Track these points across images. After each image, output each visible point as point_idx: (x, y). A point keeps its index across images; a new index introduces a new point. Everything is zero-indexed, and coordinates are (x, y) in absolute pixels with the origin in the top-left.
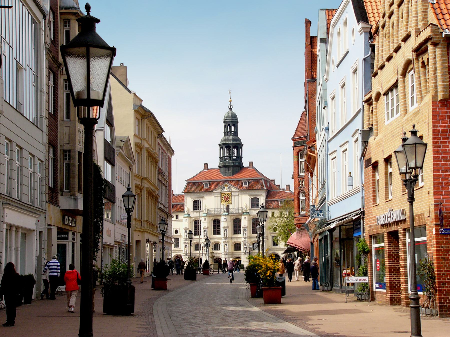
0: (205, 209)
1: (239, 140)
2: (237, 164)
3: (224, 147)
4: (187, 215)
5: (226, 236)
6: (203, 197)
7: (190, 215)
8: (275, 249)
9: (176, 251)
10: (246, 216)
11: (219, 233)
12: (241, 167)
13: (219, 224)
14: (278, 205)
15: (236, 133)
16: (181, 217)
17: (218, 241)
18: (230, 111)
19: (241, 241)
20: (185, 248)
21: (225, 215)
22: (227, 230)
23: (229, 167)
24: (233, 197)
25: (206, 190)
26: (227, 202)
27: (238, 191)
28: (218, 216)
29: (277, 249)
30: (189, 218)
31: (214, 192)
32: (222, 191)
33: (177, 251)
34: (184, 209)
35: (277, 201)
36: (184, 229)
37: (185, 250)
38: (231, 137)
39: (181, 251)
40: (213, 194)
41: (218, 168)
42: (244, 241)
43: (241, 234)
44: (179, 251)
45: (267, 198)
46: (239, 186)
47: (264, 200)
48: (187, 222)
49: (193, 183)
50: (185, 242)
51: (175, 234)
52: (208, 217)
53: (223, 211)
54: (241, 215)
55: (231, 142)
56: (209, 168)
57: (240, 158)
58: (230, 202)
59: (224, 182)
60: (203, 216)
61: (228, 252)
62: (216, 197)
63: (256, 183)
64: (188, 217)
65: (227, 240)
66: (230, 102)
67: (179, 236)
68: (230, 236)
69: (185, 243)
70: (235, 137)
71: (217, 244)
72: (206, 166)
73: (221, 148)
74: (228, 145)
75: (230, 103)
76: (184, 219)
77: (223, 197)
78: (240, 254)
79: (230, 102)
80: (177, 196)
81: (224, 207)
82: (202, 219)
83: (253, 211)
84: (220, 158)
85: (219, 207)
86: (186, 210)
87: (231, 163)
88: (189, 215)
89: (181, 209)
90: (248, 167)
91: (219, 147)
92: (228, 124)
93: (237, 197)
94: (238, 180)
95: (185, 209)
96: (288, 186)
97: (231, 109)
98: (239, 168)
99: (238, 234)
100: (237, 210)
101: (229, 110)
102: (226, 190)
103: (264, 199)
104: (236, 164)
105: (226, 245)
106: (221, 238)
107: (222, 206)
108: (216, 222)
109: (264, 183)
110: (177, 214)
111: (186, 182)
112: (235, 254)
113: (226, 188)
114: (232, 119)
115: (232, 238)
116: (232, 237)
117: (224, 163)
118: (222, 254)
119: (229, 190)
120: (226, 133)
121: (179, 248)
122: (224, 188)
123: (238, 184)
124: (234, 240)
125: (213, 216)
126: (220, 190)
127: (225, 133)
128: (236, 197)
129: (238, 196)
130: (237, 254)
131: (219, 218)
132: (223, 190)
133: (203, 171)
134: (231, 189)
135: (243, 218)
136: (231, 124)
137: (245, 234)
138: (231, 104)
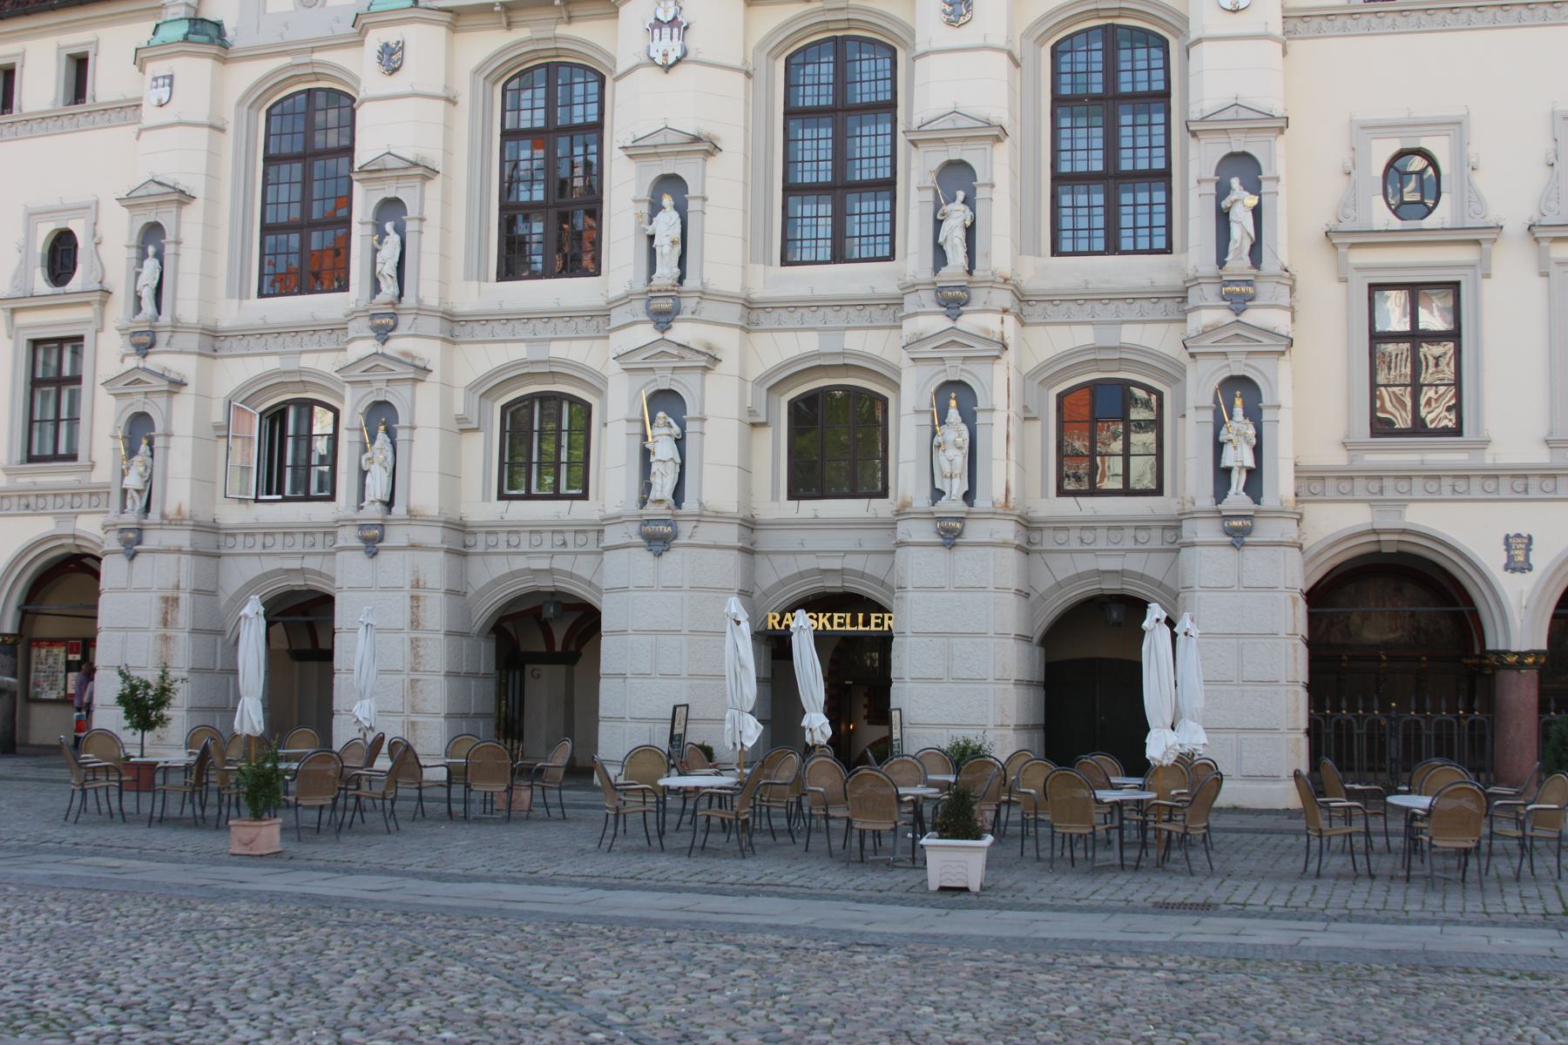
5: (667, 269)
7: (218, 26)
8: (1405, 476)
17: (558, 350)
20: (132, 452)
29: (1434, 476)
36: (130, 201)
37: (133, 481)
50: (132, 380)
52: (439, 32)
105: (666, 401)
110: (76, 40)
112: (790, 540)
116: (759, 292)
118: (613, 536)
130: (814, 541)
137: (953, 235)
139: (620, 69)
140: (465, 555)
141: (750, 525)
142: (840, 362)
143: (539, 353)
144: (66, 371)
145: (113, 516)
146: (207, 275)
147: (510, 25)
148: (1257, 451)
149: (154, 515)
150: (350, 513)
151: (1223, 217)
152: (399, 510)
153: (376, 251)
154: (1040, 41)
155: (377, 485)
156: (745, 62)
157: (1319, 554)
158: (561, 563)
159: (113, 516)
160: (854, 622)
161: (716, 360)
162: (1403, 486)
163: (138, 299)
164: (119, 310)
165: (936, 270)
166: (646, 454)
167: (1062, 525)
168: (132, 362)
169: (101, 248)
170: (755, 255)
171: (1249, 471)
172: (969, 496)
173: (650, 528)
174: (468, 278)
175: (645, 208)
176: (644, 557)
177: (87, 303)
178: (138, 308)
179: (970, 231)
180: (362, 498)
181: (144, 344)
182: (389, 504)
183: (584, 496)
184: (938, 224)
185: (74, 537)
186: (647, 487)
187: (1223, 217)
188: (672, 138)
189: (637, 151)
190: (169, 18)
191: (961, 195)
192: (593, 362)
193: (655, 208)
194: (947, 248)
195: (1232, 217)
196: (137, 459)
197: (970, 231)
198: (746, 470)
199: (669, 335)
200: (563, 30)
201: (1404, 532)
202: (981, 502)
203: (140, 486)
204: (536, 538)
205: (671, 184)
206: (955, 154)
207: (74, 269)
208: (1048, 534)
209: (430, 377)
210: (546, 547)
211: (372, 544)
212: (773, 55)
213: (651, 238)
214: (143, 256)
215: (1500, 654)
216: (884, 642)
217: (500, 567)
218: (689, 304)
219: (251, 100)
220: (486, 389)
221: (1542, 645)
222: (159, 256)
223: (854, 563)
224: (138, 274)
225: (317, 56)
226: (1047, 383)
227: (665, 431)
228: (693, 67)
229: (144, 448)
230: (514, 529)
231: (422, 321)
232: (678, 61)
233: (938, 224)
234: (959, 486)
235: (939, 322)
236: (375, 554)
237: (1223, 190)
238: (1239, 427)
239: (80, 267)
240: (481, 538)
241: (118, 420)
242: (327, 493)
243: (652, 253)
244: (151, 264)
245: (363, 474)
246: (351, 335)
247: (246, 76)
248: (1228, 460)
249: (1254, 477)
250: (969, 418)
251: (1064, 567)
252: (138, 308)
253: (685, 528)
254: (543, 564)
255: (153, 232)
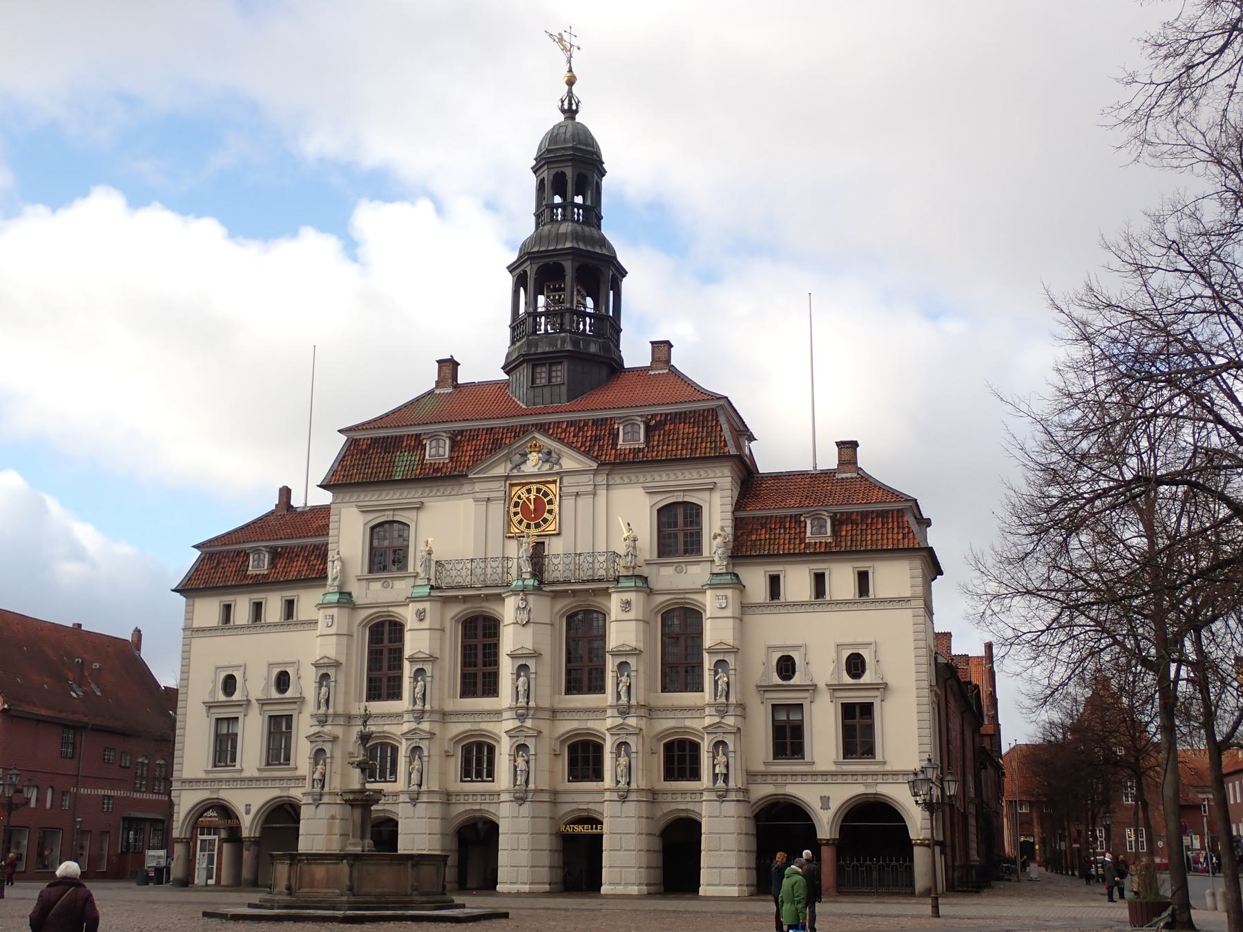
0: (427, 564)
1: (603, 242)
2: (593, 348)
3: (530, 269)
4: (335, 598)
6: (420, 507)
7: (350, 594)
8: (784, 774)
9: (274, 779)
10: (631, 596)
11: (491, 689)
12: (613, 366)
13: (491, 641)
14: (802, 540)
15: (593, 215)
16: (308, 602)
18: (570, 122)
19: (604, 726)
20: (316, 763)
21: (524, 590)
22: (532, 670)
23: (550, 360)
24: (568, 503)
25: (436, 470)
26: (537, 526)
27: (596, 472)
28: (488, 597)
29: (794, 775)
30: (346, 612)
31: (472, 481)
32: (515, 472)
33: (281, 779)
34: (325, 570)
35: (796, 519)
37: (317, 776)
38: (565, 228)
39: (297, 779)
40: (466, 488)
41: (507, 377)
42: (620, 727)
43: (601, 689)
44: (289, 779)
45: (739, 506)
46: (601, 448)
47: (729, 515)
48: (333, 630)
49: (375, 440)
50: (318, 735)
51: (275, 694)
52: (438, 605)
53: (514, 571)
54: (606, 593)
55: (568, 245)
56: (460, 381)
57: (609, 327)
58: (552, 528)
59: (525, 430)
60: (413, 599)
61: (531, 786)
62: (483, 505)
63: (684, 429)
64: (339, 604)
65: (529, 723)
66: (571, 82)
67: (293, 701)
68: (545, 703)
69: (312, 738)
70: (587, 229)
71: (480, 745)
72: (447, 370)
73: (520, 281)
74: (550, 261)
75: (566, 88)
76: (320, 615)
77: (517, 504)
78: (597, 798)
79: (571, 82)
80: (302, 513)
81: (518, 553)
82: (408, 614)
83: (667, 571)
84: (515, 326)
85: (495, 551)
86: (333, 570)
87: (564, 341)
88: (346, 600)
89: (311, 568)
90: (646, 369)
91: (508, 281)
92: (553, 172)
93: (589, 499)
94: (595, 422)
95: (330, 564)
96: (848, 448)
97: (570, 113)
98: (604, 372)
99: (591, 690)
100: (586, 566)
101: (561, 118)
102: (533, 464)
103: (729, 508)
104: (587, 344)
105: (522, 747)
106: (499, 713)
107: (512, 548)
108: (480, 632)
109: (725, 427)
111: (343, 439)
113: (534, 457)
114: (573, 148)
115: (554, 713)
116: (557, 706)
117: (529, 344)
118: (504, 797)
119: (547, 466)
120: (544, 212)
121: (292, 764)
122: (524, 455)
123: (597, 438)
124: (567, 726)
125: (465, 599)
126: (501, 470)
127: (538, 216)
128: (584, 502)
129: (594, 494)
130: (577, 798)
131: (492, 608)
132: (517, 466)
133: (431, 393)
134: (557, 463)
135: (614, 603)
136: (569, 172)
137: (623, 690)
138: (570, 92)
139: (506, 623)
140: (449, 804)
141: (555, 793)
142: (586, 731)
143: (476, 727)
144: (284, 729)
145: (308, 788)
146: (347, 693)
147: (465, 602)
148: (727, 767)
149: (326, 789)
150: (405, 788)
151: (716, 683)
152: (424, 788)
153: (415, 688)
154: (657, 613)
155: (415, 777)
156: (551, 621)
157: (756, 803)
158: (484, 807)
159: (308, 788)
160: (592, 829)
161: (540, 732)
162: (784, 778)
163: (319, 703)
164: (310, 708)
165: (618, 701)
166: (515, 767)
167: (665, 793)
168: (317, 729)
169: (301, 681)
170: (554, 692)
171: (725, 774)
172: (629, 784)
173: (517, 795)
174: (449, 697)
175: (515, 677)
176: (515, 805)
177: (296, 702)
178: (319, 708)
179: (629, 688)
180: (410, 783)
181: (323, 721)
182: (420, 785)
183: (493, 781)
184: (618, 684)
185: (289, 797)
186: (515, 780)
187: (716, 683)
188: (525, 651)
189: (513, 656)
190: (331, 591)
191: (626, 674)
192: (496, 731)
193: (518, 676)
194: (622, 693)
195: (720, 683)
196: (319, 767)
197: (629, 688)
198: (552, 772)
199: (523, 724)
200: (485, 604)
201: (785, 795)
202: (633, 786)
203: (320, 778)
204: (475, 798)
205: (523, 667)
206: (623, 659)
207: (289, 686)
208: (660, 796)
209: (436, 737)
210: (479, 801)
211: (414, 801)
212: (561, 616)
213: (517, 688)
214: (321, 686)
215: (821, 840)
216: (600, 837)
217: (461, 808)
218: (531, 712)
219: (363, 624)
220: (456, 740)
221: (838, 837)
222: (328, 686)
223: (591, 806)
224: (319, 693)
225: (390, 609)
226: (659, 740)
227: (522, 758)
228: (532, 625)
229: (321, 762)
230: (466, 794)
231: (433, 715)
232: (527, 622)
233: (618, 684)
234: (623, 781)
235: (620, 721)
236: (415, 805)
237: (716, 673)
238: (721, 759)
239: (291, 687)
240: (454, 797)
241: (311, 750)
242: (393, 779)
243: (517, 693)
244: (324, 689)
245: (410, 774)
246: (405, 719)
247: (364, 614)
248: (717, 771)
249: (726, 777)
250: (628, 754)
251: (666, 808)
252: (319, 708)
253: (530, 795)
254: (477, 807)
255: (325, 677)
